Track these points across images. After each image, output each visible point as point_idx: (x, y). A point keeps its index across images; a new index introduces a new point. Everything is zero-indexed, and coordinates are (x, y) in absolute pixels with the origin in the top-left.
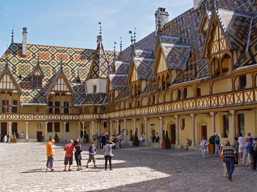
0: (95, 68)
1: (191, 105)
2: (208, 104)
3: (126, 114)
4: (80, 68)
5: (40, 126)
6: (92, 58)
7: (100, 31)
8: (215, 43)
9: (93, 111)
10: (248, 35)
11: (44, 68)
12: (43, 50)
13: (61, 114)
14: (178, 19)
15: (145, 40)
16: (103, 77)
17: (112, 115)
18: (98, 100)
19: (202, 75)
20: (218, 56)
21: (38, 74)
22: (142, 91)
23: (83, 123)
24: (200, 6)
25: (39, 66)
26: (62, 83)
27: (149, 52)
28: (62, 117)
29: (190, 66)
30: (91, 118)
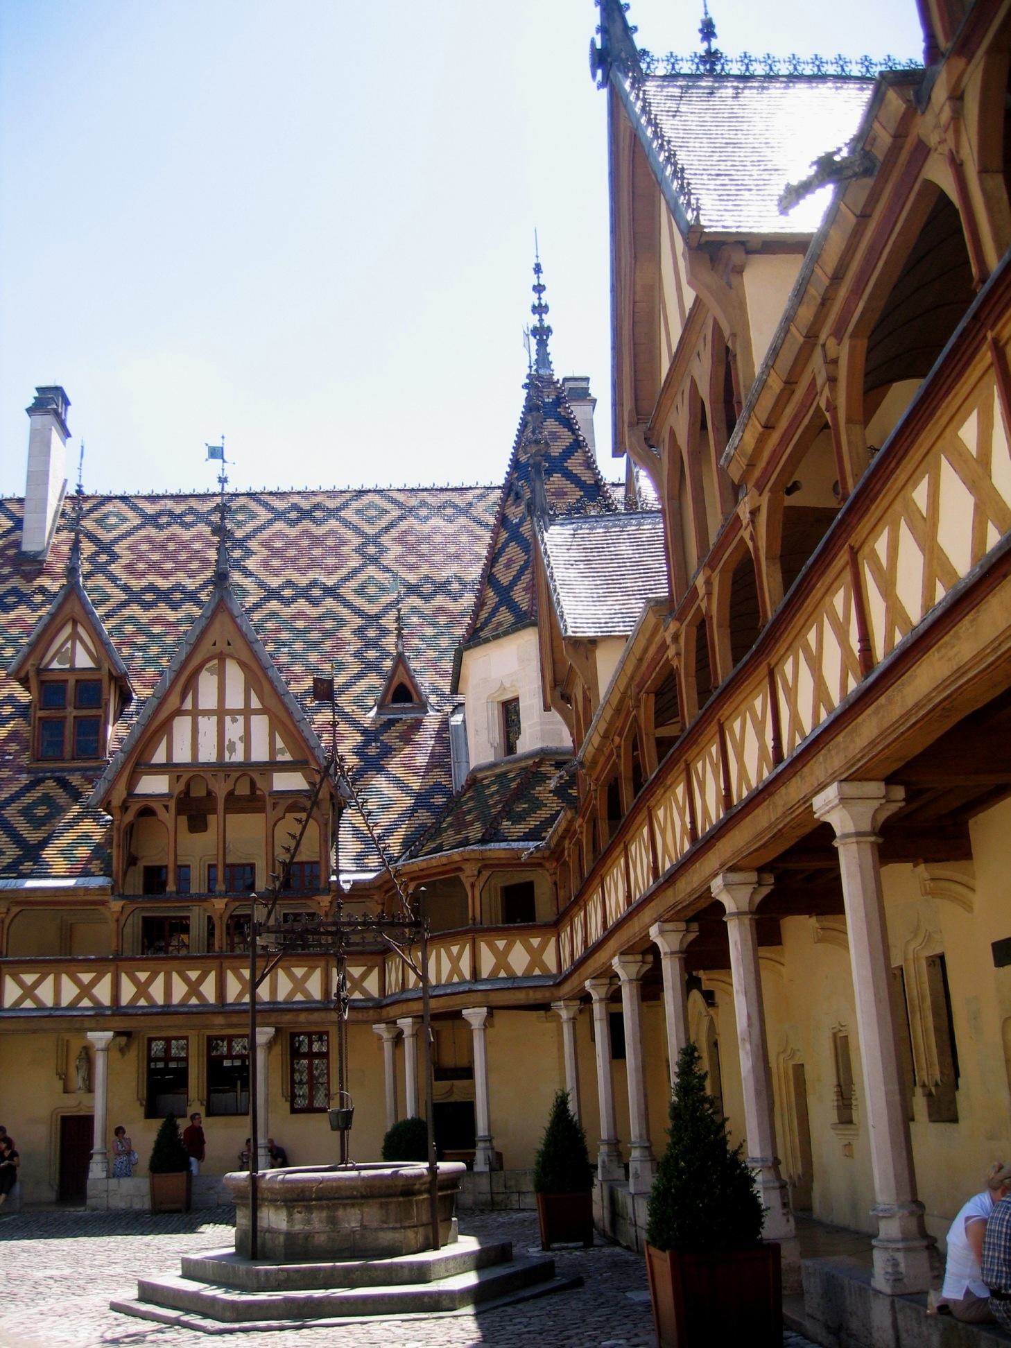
5: (83, 1073)
7: (533, 298)
11: (157, 630)
23: (406, 1024)
26: (235, 699)
30: (461, 975)
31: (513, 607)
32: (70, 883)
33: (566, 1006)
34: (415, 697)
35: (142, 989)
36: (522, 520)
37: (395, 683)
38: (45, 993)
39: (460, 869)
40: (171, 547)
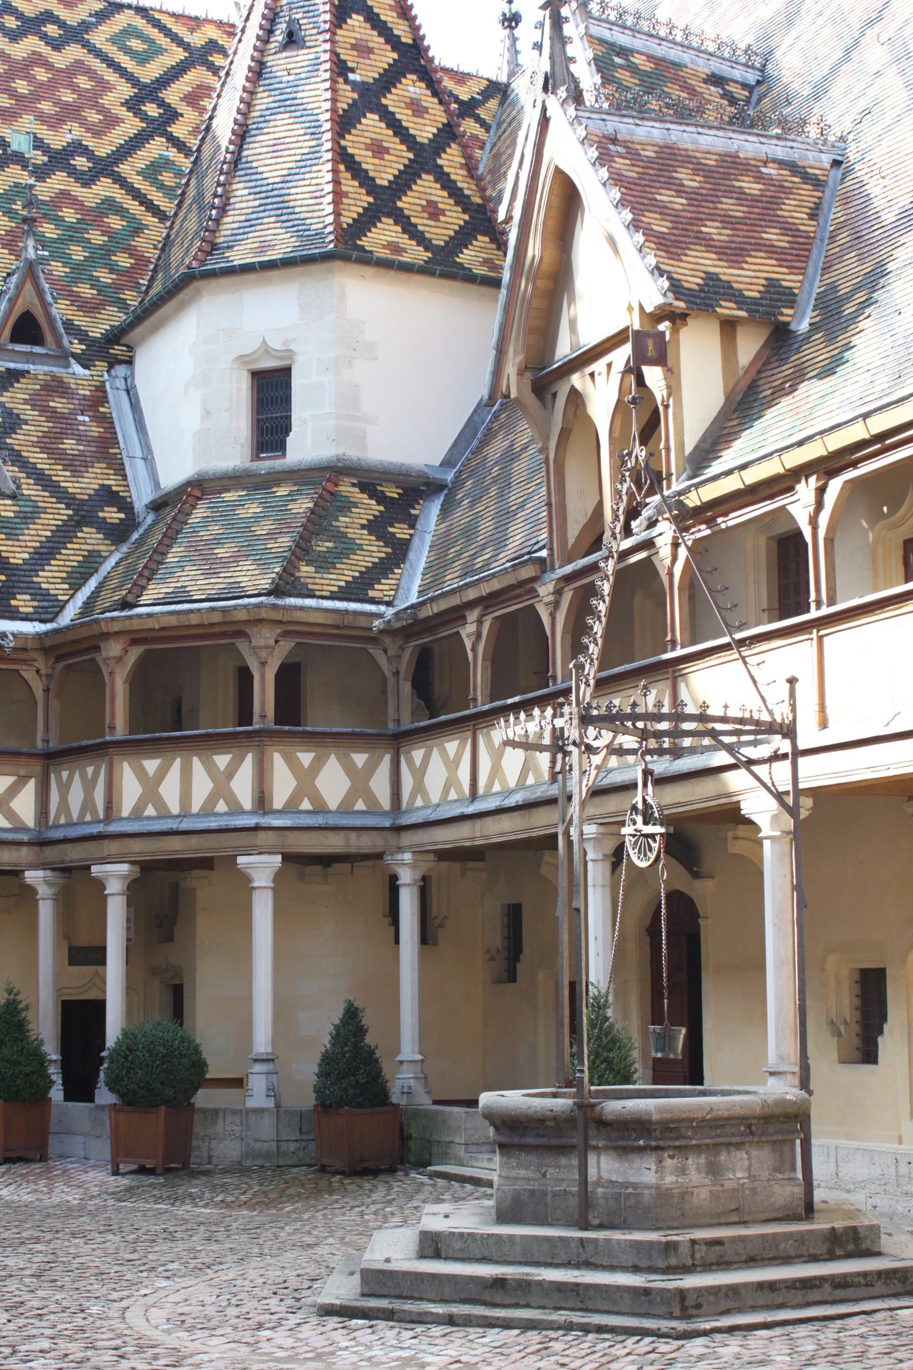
4: (46, 190)
16: (385, 254)
33: (413, 866)
34: (49, 338)
37: (18, 310)
39: (241, 634)
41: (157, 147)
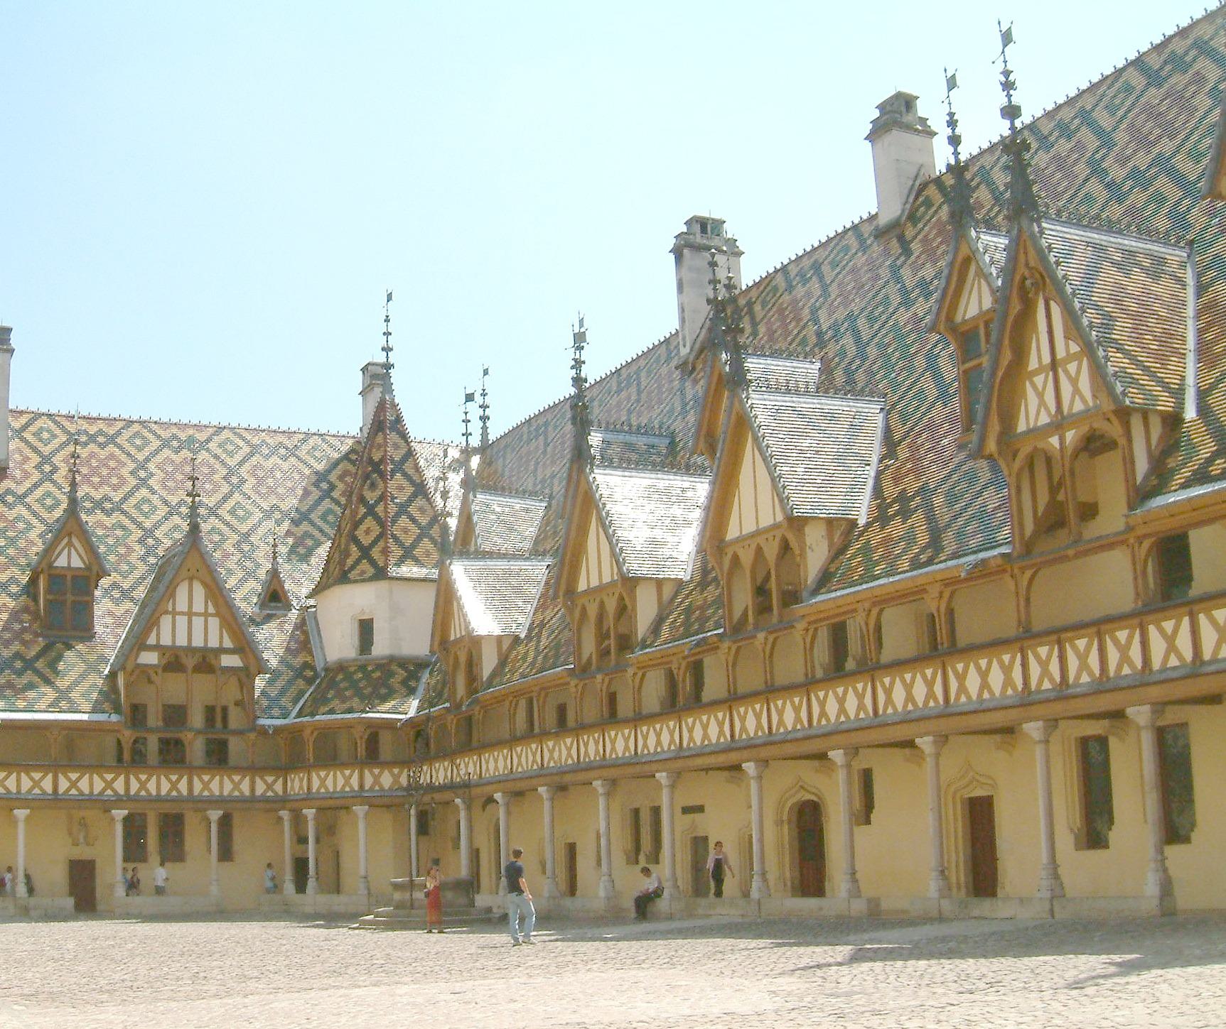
0: (363, 527)
1: (920, 691)
2: (1008, 682)
3: (551, 758)
6: (341, 478)
8: (1035, 379)
9: (361, 751)
10: (1184, 340)
12: (92, 439)
13: (191, 770)
14: (793, 270)
15: (619, 383)
17: (468, 767)
18: (383, 691)
19: (973, 543)
20: (1054, 441)
21: (70, 559)
22: (640, 637)
23: (310, 813)
24: (908, 206)
25: (78, 519)
26: (199, 606)
27: (655, 441)
28: (198, 786)
29: (894, 501)
31: (373, 563)
32: (85, 717)
35: (143, 785)
36: (377, 502)
38: (84, 785)
40: (94, 463)
41: (327, 503)
